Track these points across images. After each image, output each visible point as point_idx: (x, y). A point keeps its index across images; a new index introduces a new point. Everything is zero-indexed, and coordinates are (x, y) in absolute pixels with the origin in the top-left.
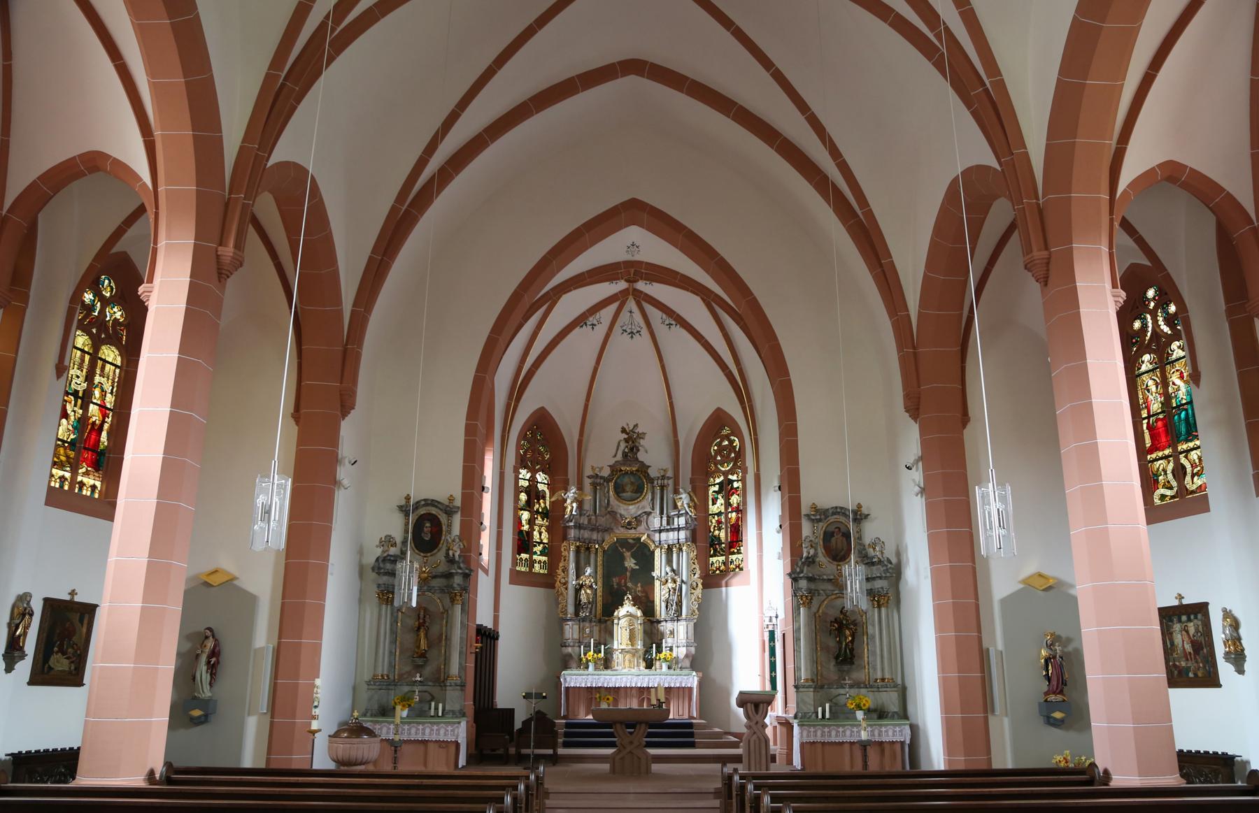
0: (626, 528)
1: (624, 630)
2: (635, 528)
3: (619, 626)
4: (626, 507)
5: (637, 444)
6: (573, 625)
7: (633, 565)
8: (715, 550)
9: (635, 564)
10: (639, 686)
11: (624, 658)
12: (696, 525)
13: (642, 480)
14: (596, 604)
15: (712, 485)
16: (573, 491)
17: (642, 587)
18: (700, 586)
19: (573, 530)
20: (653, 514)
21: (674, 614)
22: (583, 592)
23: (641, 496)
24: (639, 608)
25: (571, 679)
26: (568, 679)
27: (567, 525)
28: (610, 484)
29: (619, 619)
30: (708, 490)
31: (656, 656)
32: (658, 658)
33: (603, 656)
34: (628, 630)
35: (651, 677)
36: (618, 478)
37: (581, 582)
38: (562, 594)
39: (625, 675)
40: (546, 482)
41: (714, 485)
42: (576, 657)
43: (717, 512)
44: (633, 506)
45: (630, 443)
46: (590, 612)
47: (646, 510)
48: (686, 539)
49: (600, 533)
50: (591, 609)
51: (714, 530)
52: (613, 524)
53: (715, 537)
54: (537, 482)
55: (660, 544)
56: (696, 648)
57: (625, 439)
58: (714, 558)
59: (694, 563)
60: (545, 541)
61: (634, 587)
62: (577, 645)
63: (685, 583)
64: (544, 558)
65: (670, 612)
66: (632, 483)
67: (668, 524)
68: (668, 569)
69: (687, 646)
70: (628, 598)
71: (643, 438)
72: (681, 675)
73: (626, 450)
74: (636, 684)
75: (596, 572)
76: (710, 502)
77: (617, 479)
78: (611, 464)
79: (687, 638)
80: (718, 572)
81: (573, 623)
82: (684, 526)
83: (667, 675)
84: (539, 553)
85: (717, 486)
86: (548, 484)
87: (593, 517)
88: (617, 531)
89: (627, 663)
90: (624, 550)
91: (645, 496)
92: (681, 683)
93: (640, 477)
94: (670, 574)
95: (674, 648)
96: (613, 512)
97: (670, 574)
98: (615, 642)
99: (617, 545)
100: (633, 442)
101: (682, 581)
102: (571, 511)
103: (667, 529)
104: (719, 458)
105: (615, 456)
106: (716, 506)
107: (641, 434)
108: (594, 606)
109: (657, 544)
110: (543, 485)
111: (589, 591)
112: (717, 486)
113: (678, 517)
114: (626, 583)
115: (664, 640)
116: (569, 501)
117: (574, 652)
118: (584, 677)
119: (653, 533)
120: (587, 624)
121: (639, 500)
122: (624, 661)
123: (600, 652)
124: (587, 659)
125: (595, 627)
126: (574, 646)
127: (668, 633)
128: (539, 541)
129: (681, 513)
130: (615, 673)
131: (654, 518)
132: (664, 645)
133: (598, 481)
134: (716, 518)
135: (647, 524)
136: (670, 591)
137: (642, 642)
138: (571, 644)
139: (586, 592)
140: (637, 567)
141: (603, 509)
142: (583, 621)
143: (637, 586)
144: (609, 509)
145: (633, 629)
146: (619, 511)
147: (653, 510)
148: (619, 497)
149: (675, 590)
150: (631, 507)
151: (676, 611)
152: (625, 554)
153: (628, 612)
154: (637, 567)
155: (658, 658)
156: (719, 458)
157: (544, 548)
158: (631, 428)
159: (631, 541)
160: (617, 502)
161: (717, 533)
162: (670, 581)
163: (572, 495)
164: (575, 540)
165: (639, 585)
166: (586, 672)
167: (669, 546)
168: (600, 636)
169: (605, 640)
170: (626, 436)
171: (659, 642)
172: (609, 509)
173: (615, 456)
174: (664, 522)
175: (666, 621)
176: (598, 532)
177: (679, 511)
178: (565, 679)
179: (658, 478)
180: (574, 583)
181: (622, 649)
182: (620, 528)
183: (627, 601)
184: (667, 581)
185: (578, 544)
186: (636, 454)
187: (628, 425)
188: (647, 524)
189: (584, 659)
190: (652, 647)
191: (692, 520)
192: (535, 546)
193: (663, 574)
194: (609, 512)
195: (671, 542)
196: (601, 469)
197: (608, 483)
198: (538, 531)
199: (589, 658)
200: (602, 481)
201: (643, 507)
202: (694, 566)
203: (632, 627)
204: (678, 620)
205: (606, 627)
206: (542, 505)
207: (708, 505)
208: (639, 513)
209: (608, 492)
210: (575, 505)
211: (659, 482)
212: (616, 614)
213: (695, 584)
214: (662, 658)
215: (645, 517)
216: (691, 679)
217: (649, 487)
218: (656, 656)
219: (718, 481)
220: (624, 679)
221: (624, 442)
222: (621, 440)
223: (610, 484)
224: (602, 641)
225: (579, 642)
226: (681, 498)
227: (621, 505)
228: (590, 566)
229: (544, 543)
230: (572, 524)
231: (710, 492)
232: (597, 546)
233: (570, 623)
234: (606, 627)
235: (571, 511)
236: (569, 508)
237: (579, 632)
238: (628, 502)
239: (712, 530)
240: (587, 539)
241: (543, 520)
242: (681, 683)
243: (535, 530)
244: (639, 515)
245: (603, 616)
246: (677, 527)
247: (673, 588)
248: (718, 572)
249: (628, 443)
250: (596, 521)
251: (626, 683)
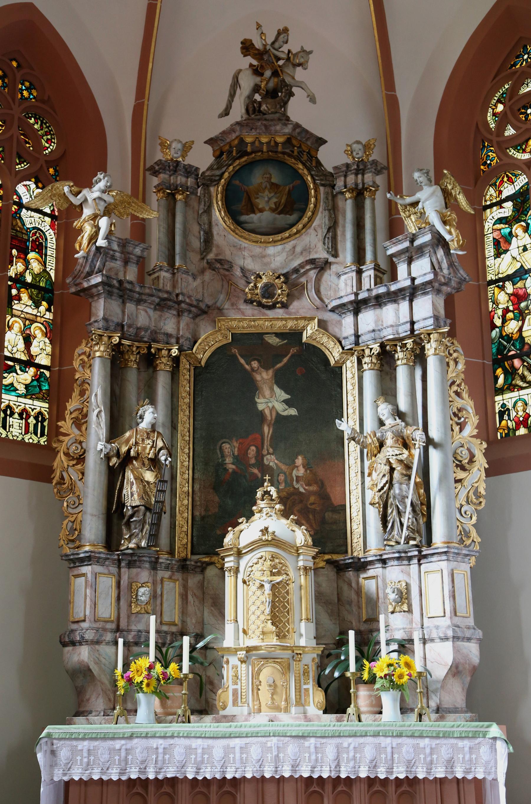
0: (260, 305)
1: (253, 588)
2: (285, 306)
3: (240, 576)
4: (257, 249)
5: (288, 80)
6: (95, 575)
7: (280, 407)
8: (511, 373)
9: (286, 402)
10: (306, 775)
11: (256, 675)
12: (462, 281)
13: (301, 177)
14: (173, 516)
15: (491, 206)
16: (102, 185)
17: (306, 466)
18: (481, 462)
19: (102, 301)
20: (334, 268)
21: (408, 539)
22: (130, 475)
23: (300, 218)
24: (298, 523)
25: (74, 751)
26: (64, 754)
27: (85, 285)
28: (212, 189)
29: (239, 554)
30: (482, 221)
31: (360, 668)
32: (366, 676)
33: (186, 669)
34: (267, 586)
35: (346, 742)
36: (236, 174)
37: (124, 449)
38: (72, 489)
39: (256, 735)
40: (48, 210)
41: (499, 204)
42: (106, 681)
43: (510, 272)
44: (279, 248)
45: (268, 73)
46: (154, 537)
47: (313, 256)
48: (436, 318)
49: (186, 319)
50: (156, 525)
51: (504, 321)
52: (222, 297)
53: (509, 338)
54: (20, 205)
55: (357, 343)
56: (481, 642)
57: (251, 65)
58: (507, 396)
59: (458, 394)
60: (44, 360)
61: (283, 467)
62: (109, 637)
63: (436, 446)
64: (41, 406)
65: (395, 532)
66: (274, 187)
67: (378, 281)
68: (384, 410)
69: (455, 638)
70: (267, 493)
71: (300, 65)
72: (446, 735)
73: (258, 97)
74: (294, 767)
75: (174, 427)
76: (490, 251)
77: (232, 177)
78: (214, 133)
79: (455, 612)
80: (522, 431)
81: (98, 568)
82: (431, 277)
83: (400, 735)
84: (22, 389)
85: (509, 205)
86: (51, 216)
87: (165, 275)
88: (233, 314)
89: (265, 694)
90: (255, 364)
91: (311, 220)
92: (450, 764)
93: (296, 171)
94: (389, 422)
95: (418, 646)
96: (220, 261)
97: (389, 422)
98: (229, 628)
99: (235, 351)
100: (275, 74)
101: (429, 442)
102: (93, 238)
103: (378, 297)
104: (510, 131)
105: (226, 113)
106: (506, 258)
107: (296, 55)
108: (165, 520)
109: (348, 344)
110: (37, 215)
111: (149, 476)
112: (509, 205)
113: (410, 261)
114: (260, 457)
115: (382, 618)
116: (87, 212)
117: (98, 662)
118: (118, 744)
119: (334, 317)
120: (144, 575)
121: (294, 230)
122: (256, 689)
123: (179, 659)
124: (130, 680)
125: (168, 585)
126: (98, 642)
127: (392, 596)
128: (24, 358)
129: (417, 243)
130: (223, 727)
131: (339, 276)
132: (383, 637)
133: (180, 179)
134: (509, 288)
135: (318, 292)
136: (392, 470)
137: (312, 626)
138: (89, 635)
139: (140, 479)
140: (293, 412)
141: (195, 258)
142: (131, 565)
143: (294, 466)
144: (211, 256)
145: (285, 584)
146: (241, 262)
147: (336, 255)
148: (239, 223)
149: (408, 467)
150: (271, 250)
151: (414, 530)
152: (258, 377)
153: (265, 531)
154: (293, 412)
155: (366, 676)
156: (510, 131)
157: (37, 378)
158: (270, 41)
159: (273, 341)
160: (233, 238)
161: (512, 327)
162: (389, 442)
163: (96, 194)
164: (107, 329)
165: (299, 461)
166: (123, 728)
167: (382, 346)
168: (184, 612)
169: (202, 623)
170: (255, 63)
171: (364, 627)
172: (211, 256)
173: (226, 113)
174: (369, 274)
175: (384, 562)
176: (179, 314)
177: (412, 241)
178: (53, 753)
179: (348, 166)
180: (99, 447)
181: (249, 650)
182: (243, 306)
183: (262, 504)
184: (381, 444)
185: (116, 340)
186: (286, 103)
187: (259, 26)
188: (318, 292)
189: (121, 683)
190: (344, 642)
191: (451, 265)
192: (11, 370)
193: (369, 425)
194: (211, 265)
195: (388, 334)
196: (186, 148)
197: (206, 186)
198: (22, 332)
199: (138, 679)
200: (190, 181)
201: (307, 250)
202: (459, 403)
203: (278, 579)
204: (421, 557)
205: (202, 586)
206: (36, 267)
207: (484, 258)
208: (296, 264)
209: (208, 210)
210: (103, 222)
211: (351, 179)
212: (228, 539)
213: (465, 452)
214: (379, 674)
215: (313, 274)
216: (484, 751)
217: (322, 196)
218: (360, 668)
219: (508, 190)
220: (255, 752)
221: (249, 72)
222: (240, 71)
223: (212, 189)
224: (191, 624)
225: (118, 629)
226: (415, 204)
227: (245, 243)
228: (153, 402)
229: (39, 366)
230: (97, 279)
231: (488, 225)
232: (175, 352)
233: (86, 569)
234: (202, 586)
235: (93, 238)
236: (88, 230)
237: (118, 598)
238: (263, 238)
239: (498, 322)
240: (146, 329)
241: (37, 305)
242: (450, 764)
243: (10, 328)
244: (296, 270)
245: (192, 553)
246: (408, 283)
247: (401, 461)
248: (522, 431)
249: (261, 75)
250: (174, 286)
251: (261, 762)
